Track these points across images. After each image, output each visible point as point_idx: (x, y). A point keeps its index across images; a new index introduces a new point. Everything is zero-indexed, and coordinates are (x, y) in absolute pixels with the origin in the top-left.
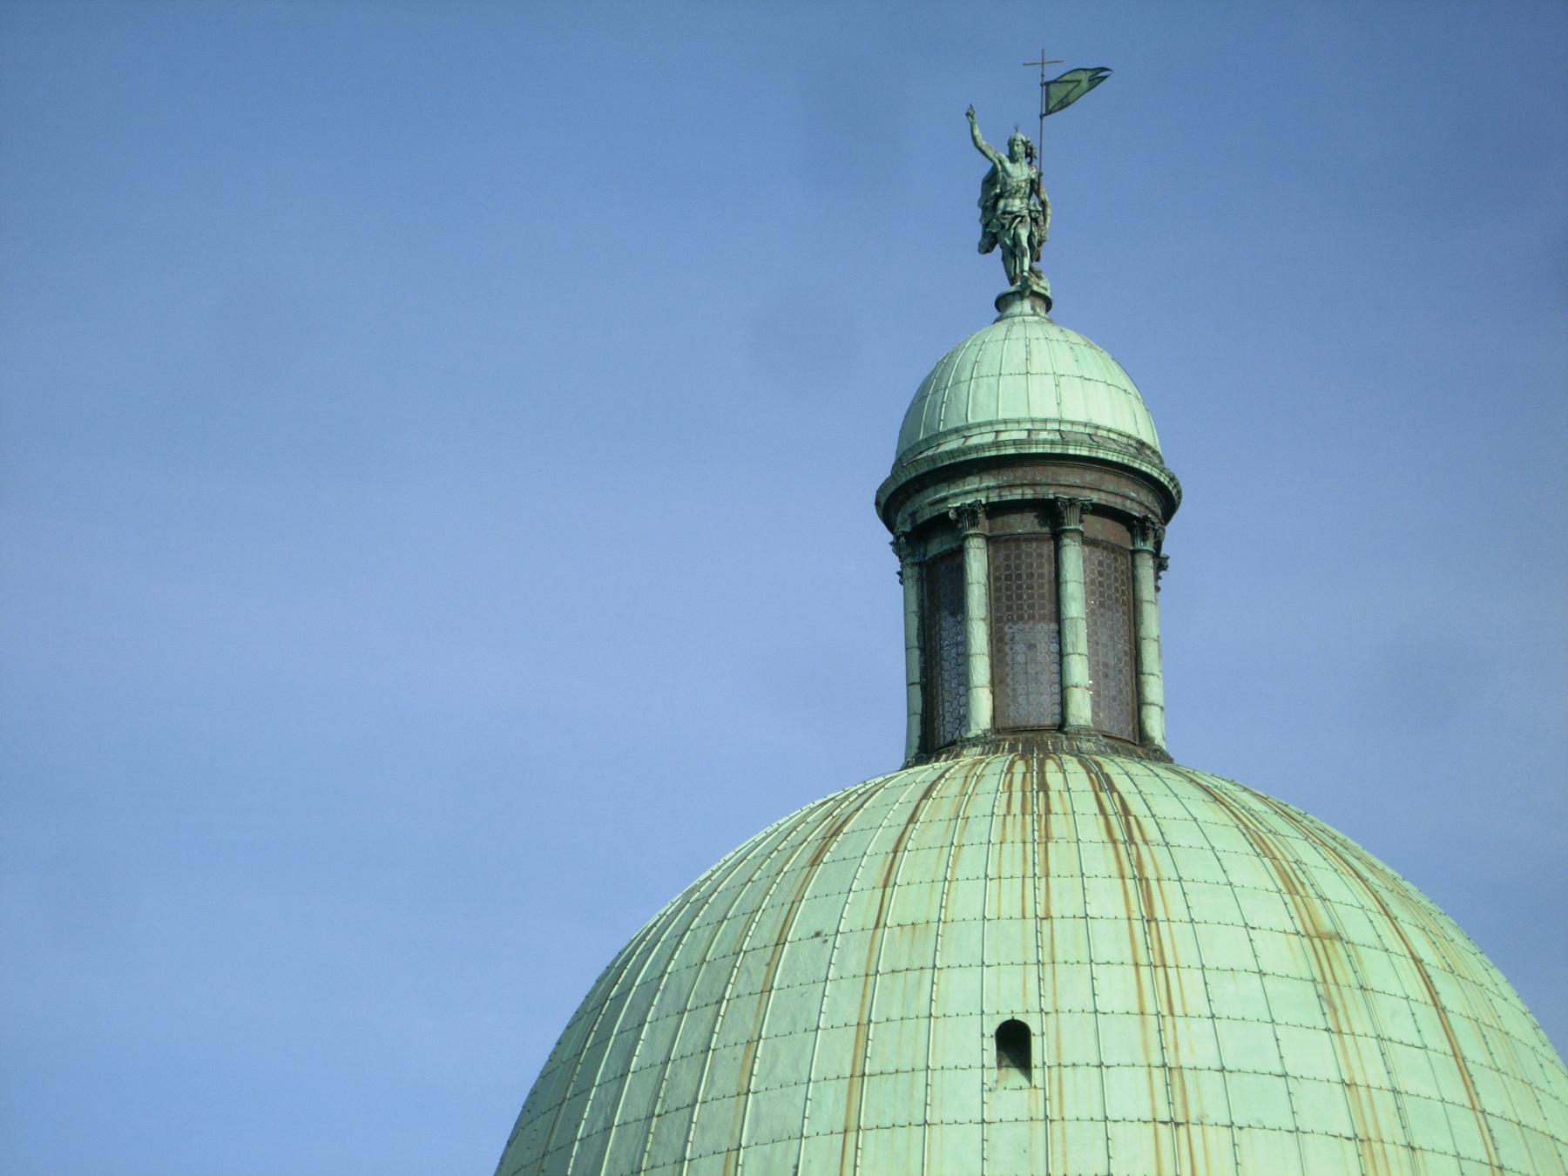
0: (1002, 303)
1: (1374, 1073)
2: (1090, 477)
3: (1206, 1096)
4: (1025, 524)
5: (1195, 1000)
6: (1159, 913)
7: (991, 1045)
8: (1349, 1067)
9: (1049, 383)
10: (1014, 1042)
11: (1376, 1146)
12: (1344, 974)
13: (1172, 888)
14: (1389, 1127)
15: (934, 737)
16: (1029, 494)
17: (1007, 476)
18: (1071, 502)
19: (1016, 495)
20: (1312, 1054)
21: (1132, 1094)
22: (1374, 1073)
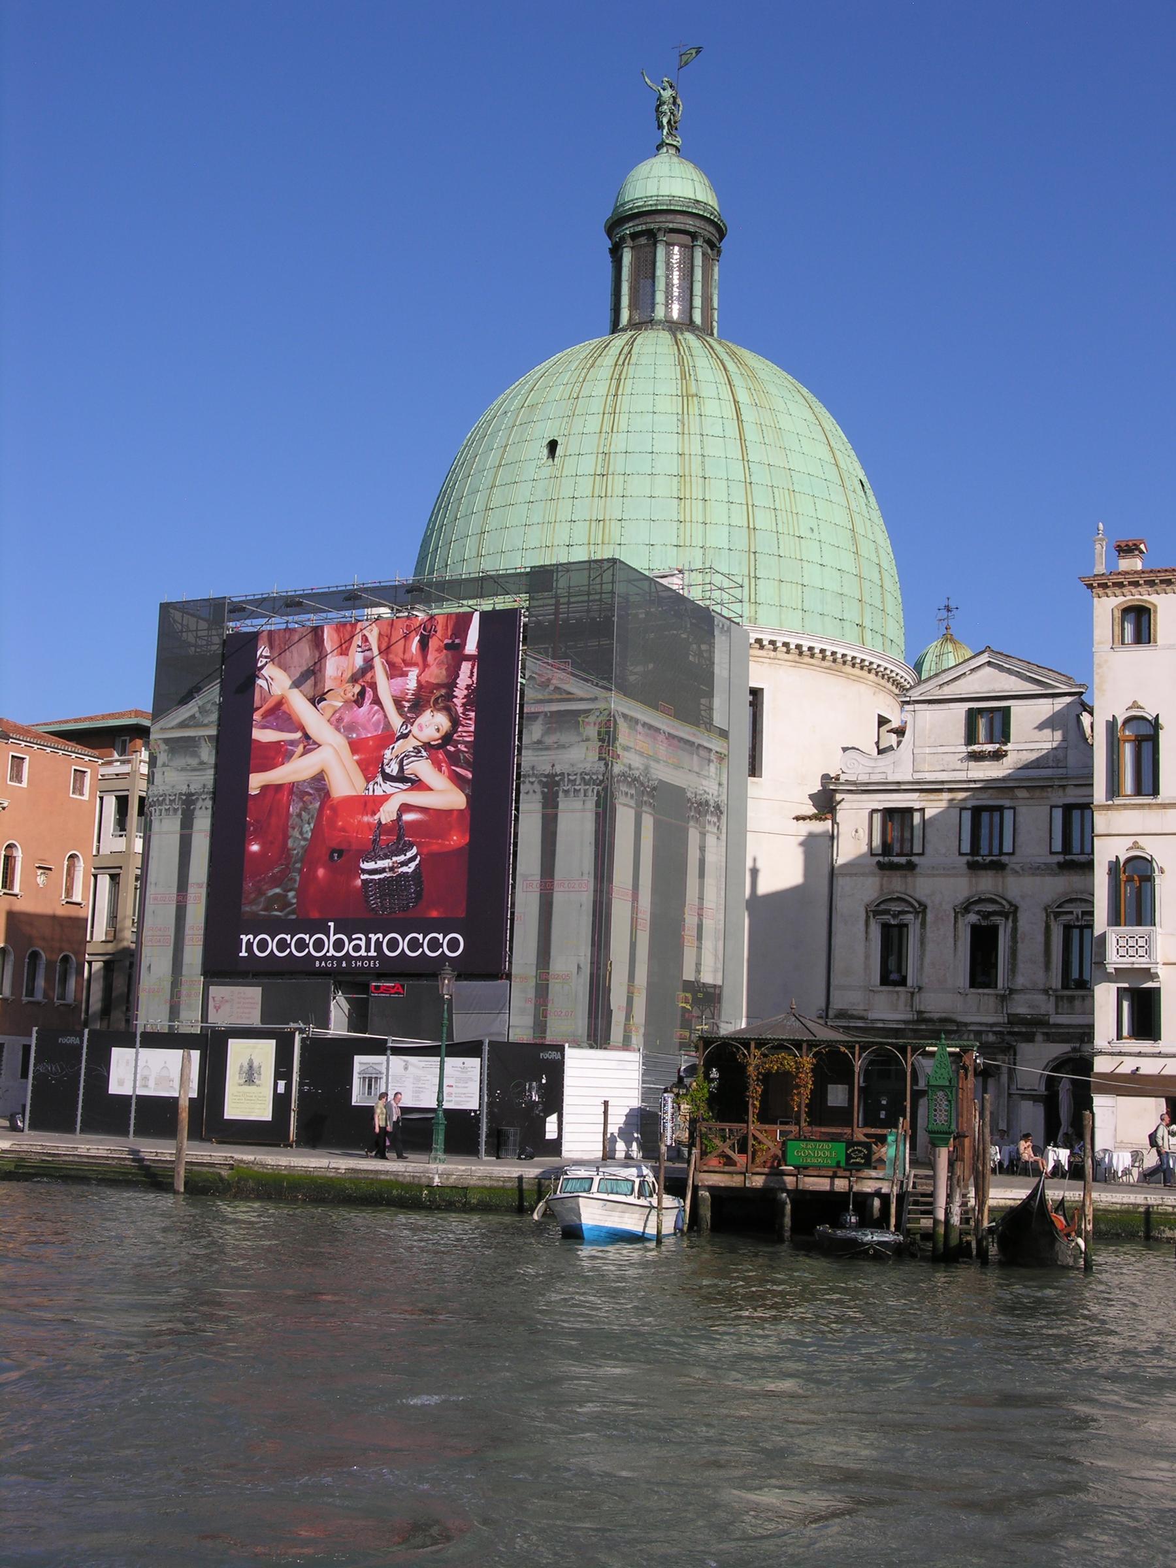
0: (659, 148)
1: (695, 448)
2: (670, 217)
3: (618, 464)
4: (643, 240)
5: (623, 426)
6: (620, 393)
7: (546, 451)
8: (683, 447)
9: (668, 180)
10: (553, 446)
11: (688, 478)
12: (694, 409)
13: (629, 382)
14: (696, 469)
15: (615, 328)
16: (644, 227)
17: (637, 222)
18: (659, 229)
19: (639, 228)
20: (671, 444)
21: (588, 465)
22: (695, 448)
